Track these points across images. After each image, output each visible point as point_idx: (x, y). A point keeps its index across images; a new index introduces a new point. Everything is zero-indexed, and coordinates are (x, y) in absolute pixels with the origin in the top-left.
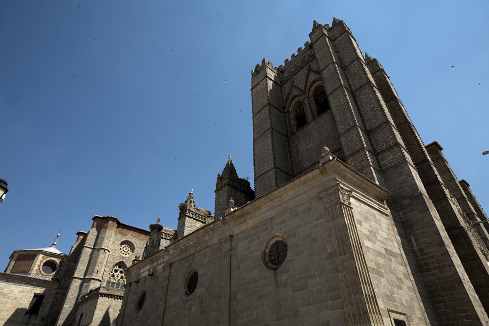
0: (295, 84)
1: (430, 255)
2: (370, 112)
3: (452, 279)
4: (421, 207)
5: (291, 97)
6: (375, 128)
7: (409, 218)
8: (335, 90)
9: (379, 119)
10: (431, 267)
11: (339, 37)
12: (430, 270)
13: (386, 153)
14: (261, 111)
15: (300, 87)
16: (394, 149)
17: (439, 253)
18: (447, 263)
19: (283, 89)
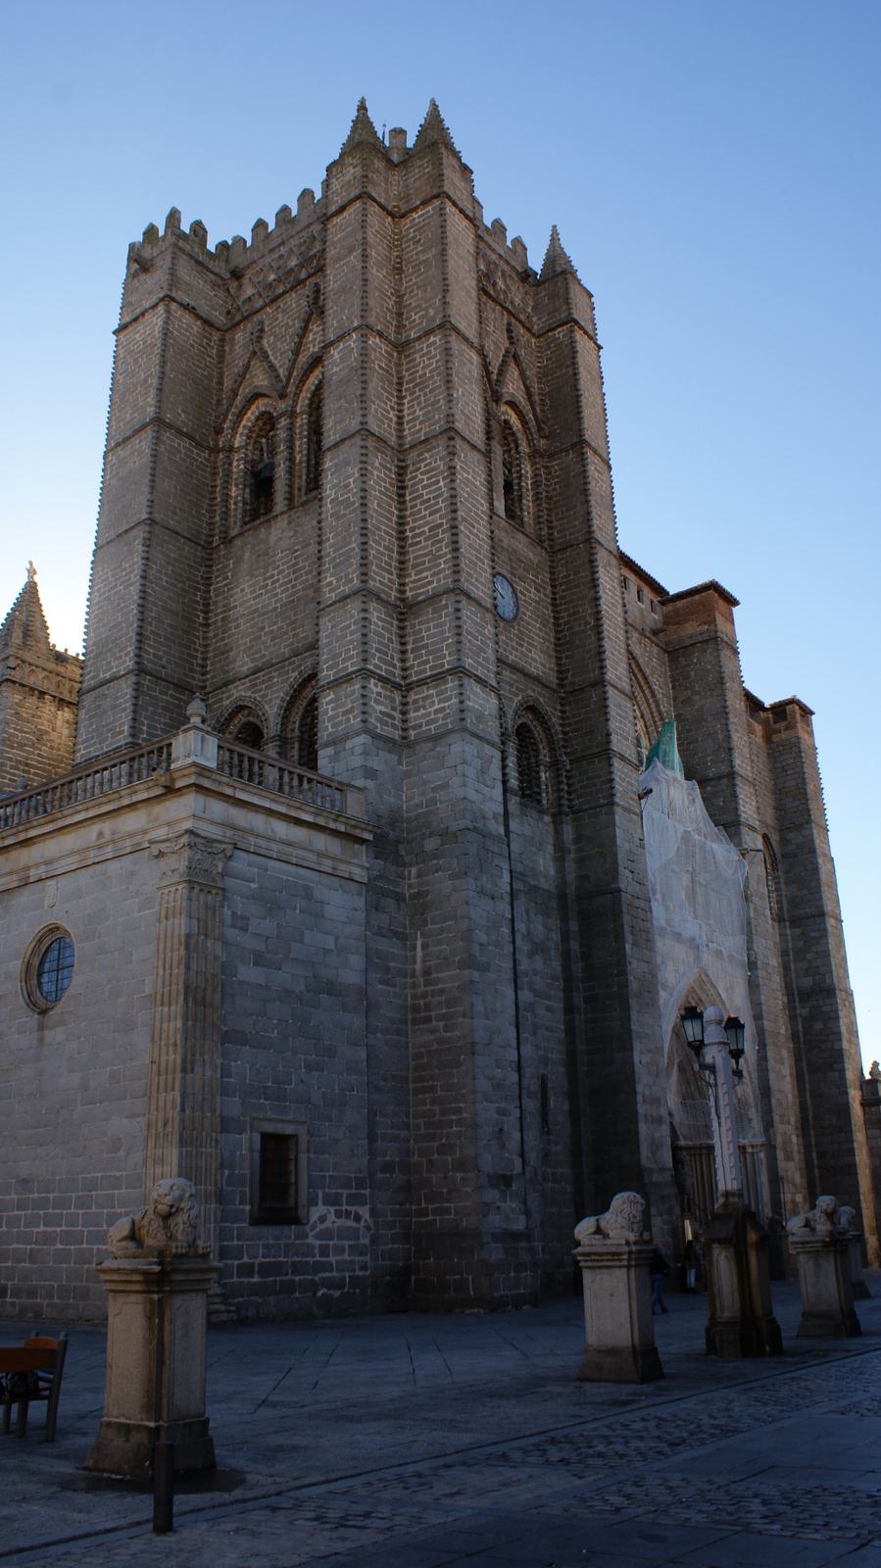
0: (265, 341)
2: (426, 540)
3: (459, 1044)
4: (455, 866)
5: (244, 392)
6: (424, 601)
8: (343, 441)
9: (440, 571)
10: (433, 1013)
11: (415, 210)
12: (429, 1020)
13: (428, 689)
14: (129, 438)
15: (275, 362)
16: (446, 682)
17: (456, 984)
18: (462, 1009)
19: (227, 348)
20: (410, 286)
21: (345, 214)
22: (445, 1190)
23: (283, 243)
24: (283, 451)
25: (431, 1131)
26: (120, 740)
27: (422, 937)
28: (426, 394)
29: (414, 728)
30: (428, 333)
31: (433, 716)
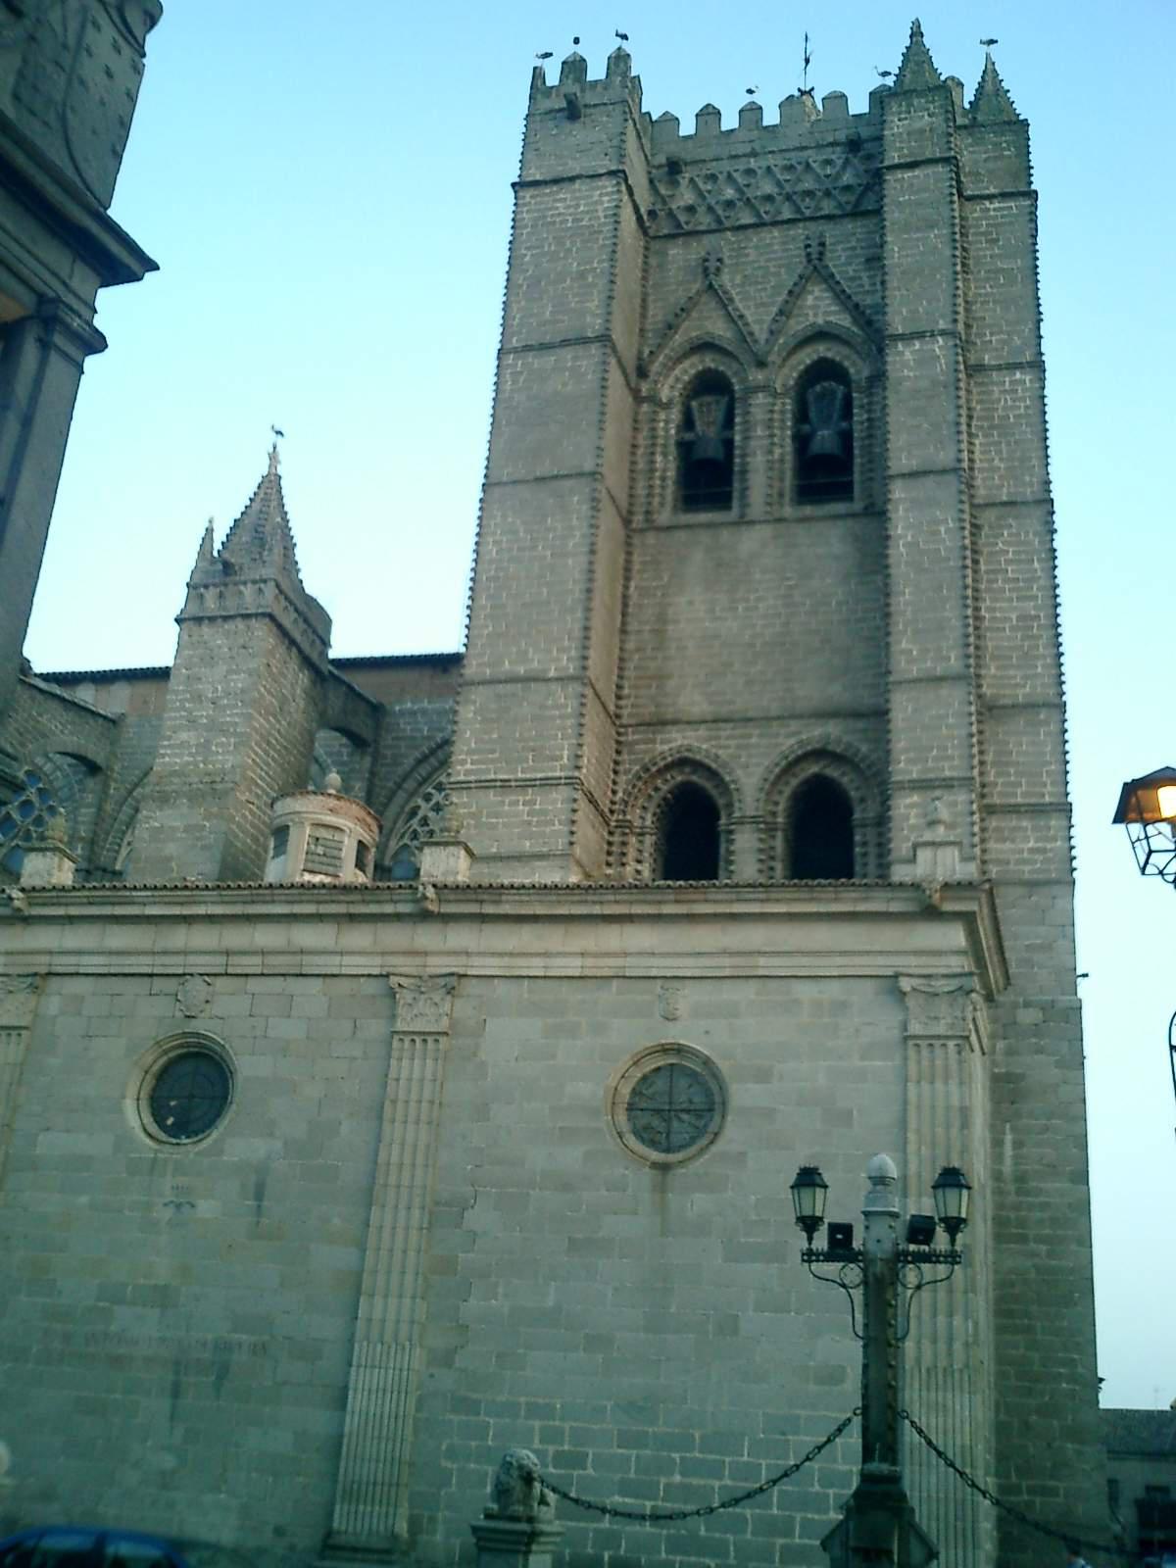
1: (1042, 1199)
7: (1019, 1071)
9: (1036, 675)
10: (1031, 1233)
11: (990, 197)
15: (747, 313)
20: (980, 295)
21: (917, 172)
22: (1049, 1464)
23: (754, 154)
24: (760, 437)
25: (1027, 1384)
26: (553, 769)
27: (1013, 1129)
28: (1008, 444)
29: (999, 862)
30: (1019, 366)
31: (1026, 855)
